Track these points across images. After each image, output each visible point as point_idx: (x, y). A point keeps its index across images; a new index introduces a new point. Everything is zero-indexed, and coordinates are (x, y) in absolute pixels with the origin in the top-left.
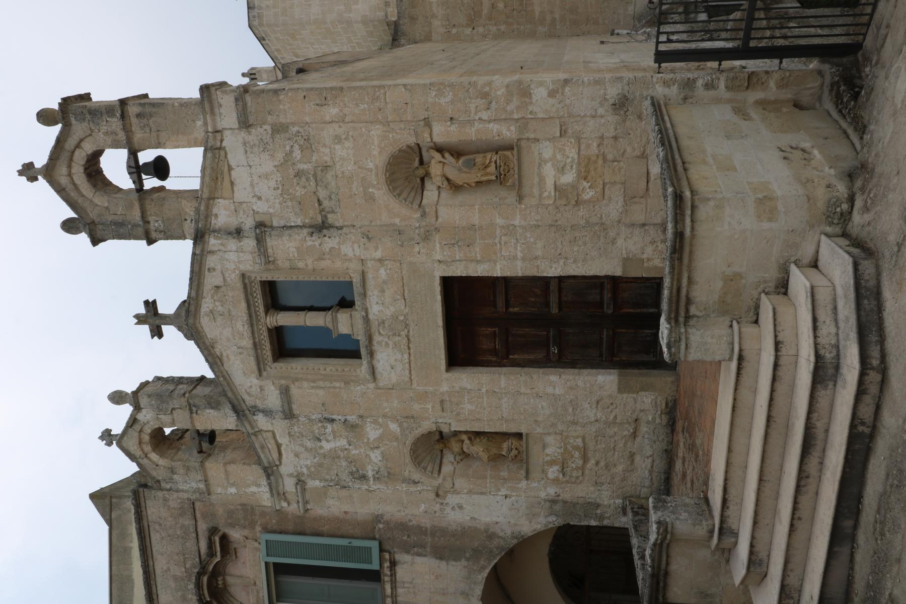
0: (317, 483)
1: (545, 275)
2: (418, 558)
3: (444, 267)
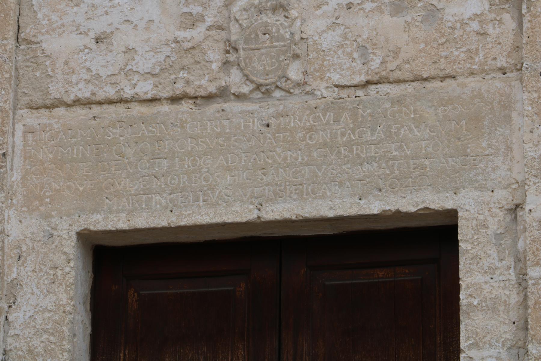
3: (493, 227)
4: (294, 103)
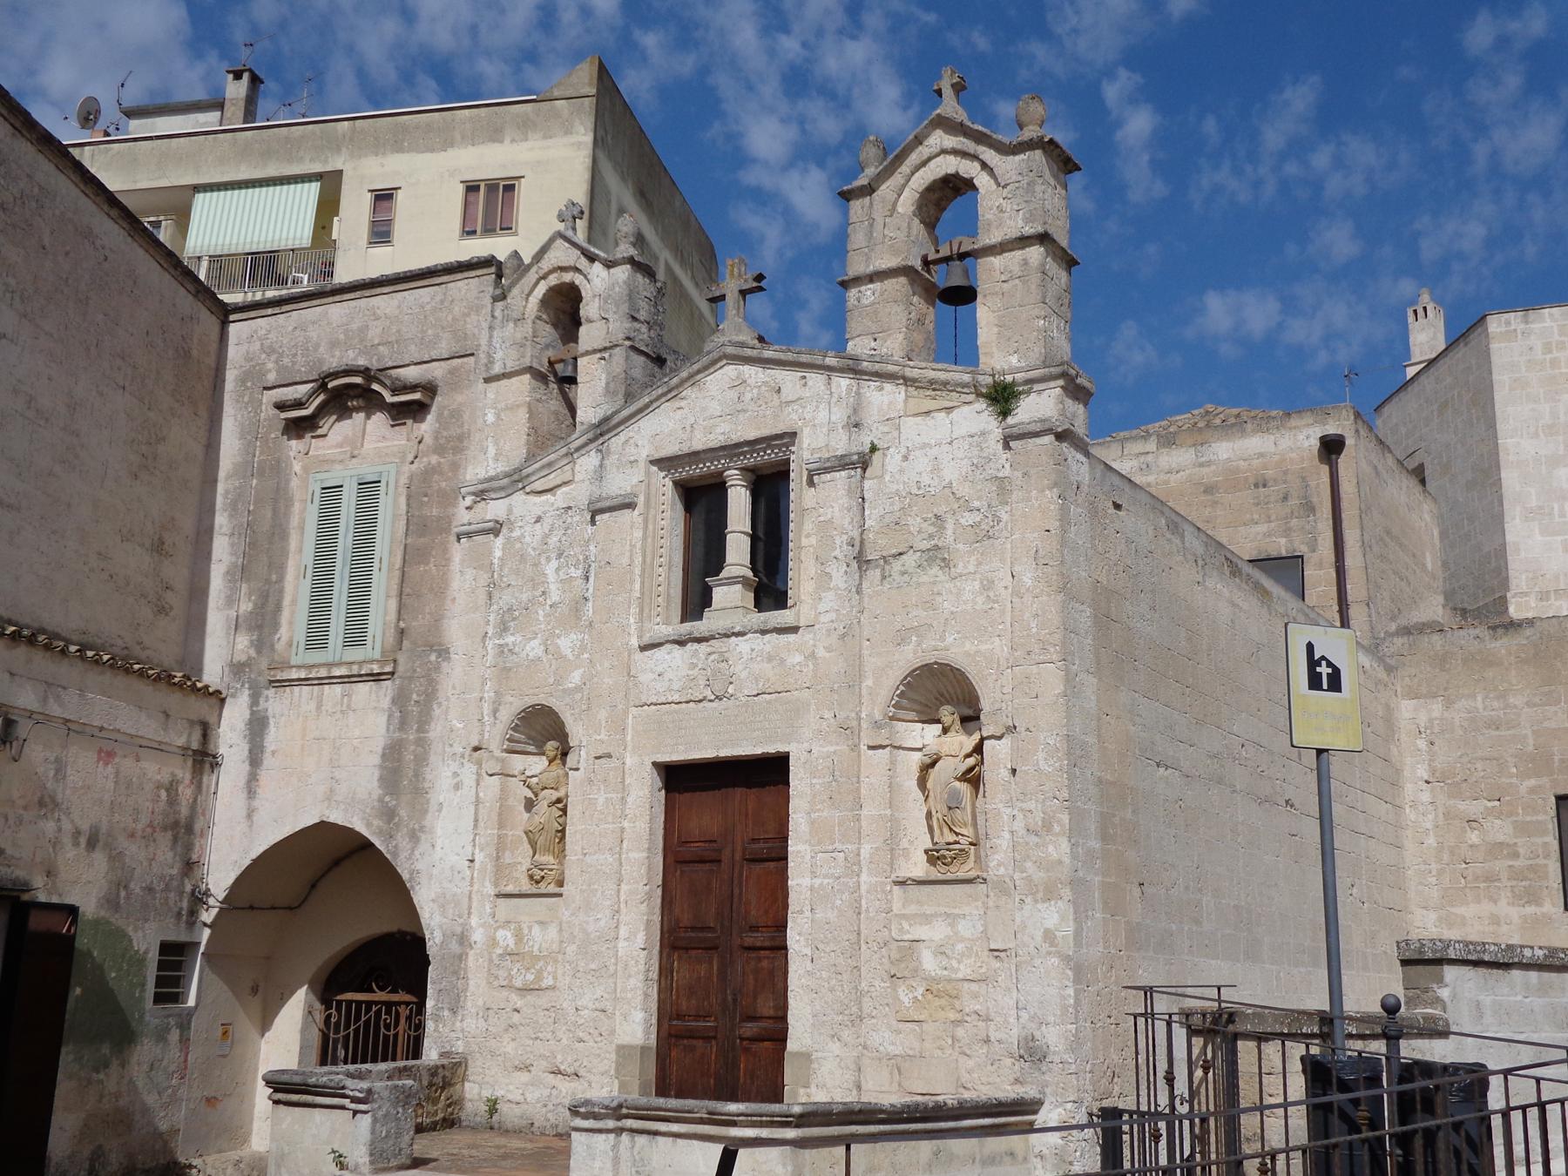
0: (498, 553)
1: (790, 924)
2: (385, 718)
4: (731, 702)
